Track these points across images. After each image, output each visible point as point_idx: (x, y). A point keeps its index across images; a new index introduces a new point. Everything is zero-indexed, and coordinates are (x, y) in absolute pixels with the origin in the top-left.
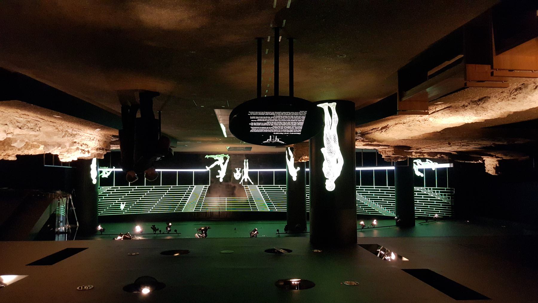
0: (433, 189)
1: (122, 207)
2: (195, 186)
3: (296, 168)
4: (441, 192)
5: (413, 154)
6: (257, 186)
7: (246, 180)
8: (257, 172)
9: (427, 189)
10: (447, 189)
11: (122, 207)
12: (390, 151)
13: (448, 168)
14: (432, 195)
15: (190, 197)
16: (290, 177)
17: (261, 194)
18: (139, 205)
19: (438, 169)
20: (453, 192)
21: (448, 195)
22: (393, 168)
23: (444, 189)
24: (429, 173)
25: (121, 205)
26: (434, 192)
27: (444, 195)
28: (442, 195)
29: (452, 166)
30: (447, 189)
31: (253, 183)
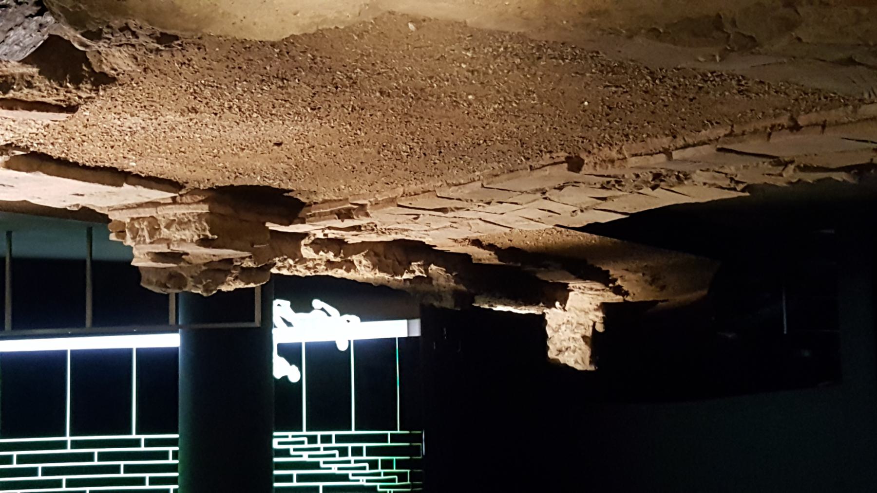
0: (339, 439)
4: (371, 451)
9: (312, 440)
10: (394, 438)
14: (334, 470)
19: (362, 347)
20: (417, 451)
21: (400, 464)
23: (384, 438)
26: (343, 452)
27: (387, 464)
28: (373, 465)
29: (416, 332)
30: (394, 438)
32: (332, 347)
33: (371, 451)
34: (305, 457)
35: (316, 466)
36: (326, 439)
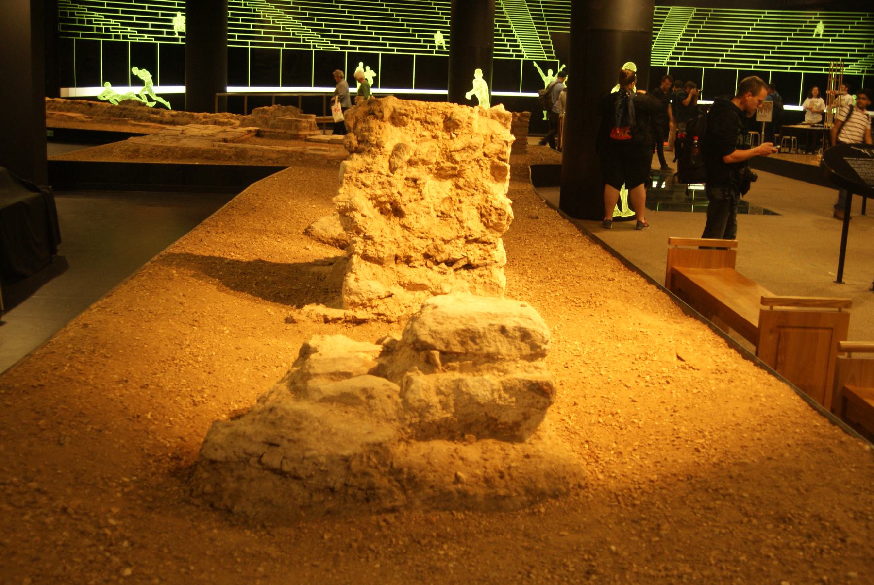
0: (110, 37)
1: (820, 28)
2: (664, 64)
3: (474, 97)
4: (92, 29)
5: (238, 123)
6: (526, 58)
7: (550, 72)
8: (416, 88)
11: (820, 28)
12: (305, 128)
13: (73, 86)
14: (113, 21)
15: (678, 41)
16: (486, 77)
17: (517, 37)
18: (785, 28)
19: (97, 84)
21: (74, 21)
22: (231, 90)
23: (83, 35)
24: (120, 78)
25: (821, 33)
26: (107, 30)
27: (82, 22)
28: (90, 22)
31: (535, 64)
32: (113, 85)
33: (92, 29)
34: (129, 29)
35: (123, 24)
36: (117, 37)
